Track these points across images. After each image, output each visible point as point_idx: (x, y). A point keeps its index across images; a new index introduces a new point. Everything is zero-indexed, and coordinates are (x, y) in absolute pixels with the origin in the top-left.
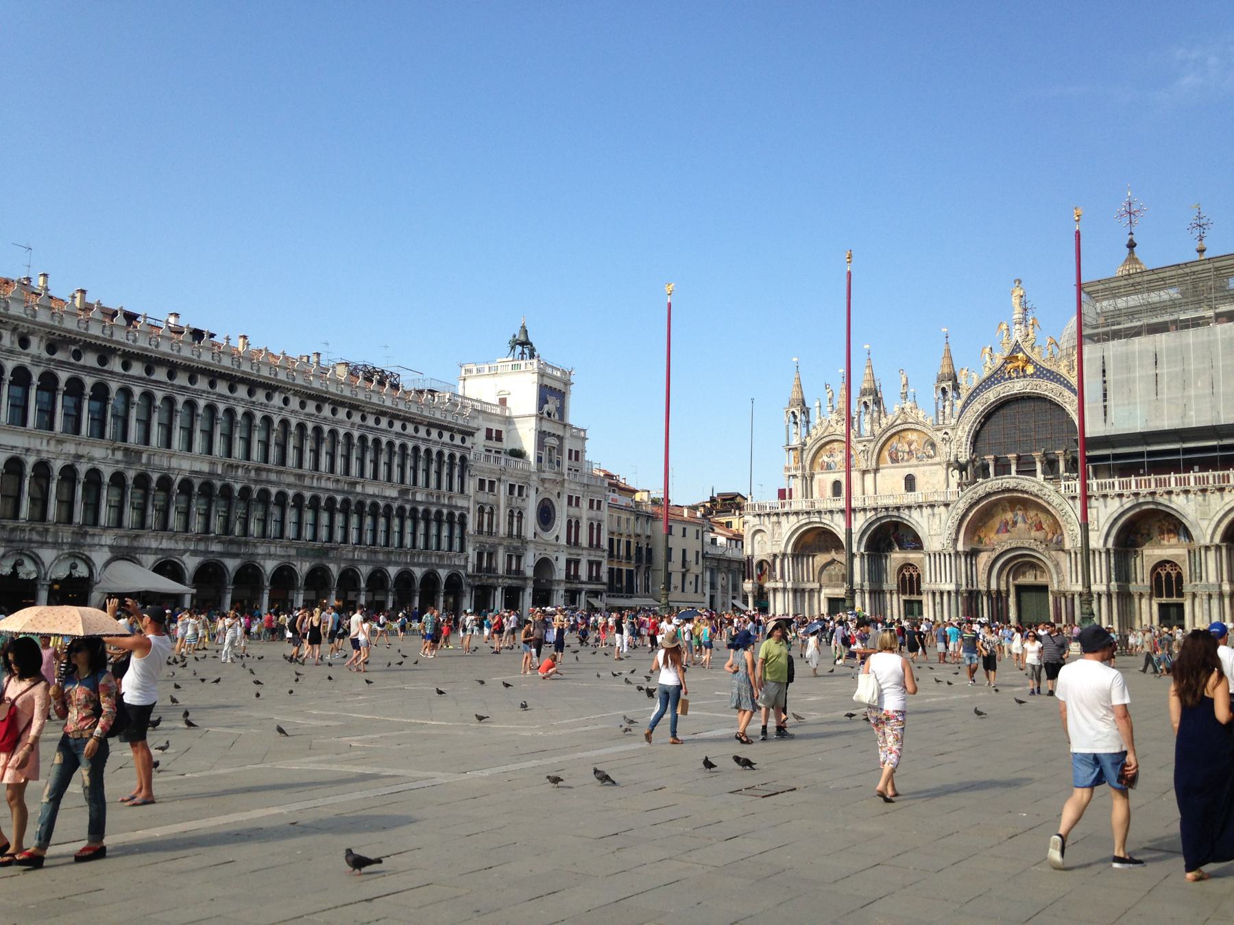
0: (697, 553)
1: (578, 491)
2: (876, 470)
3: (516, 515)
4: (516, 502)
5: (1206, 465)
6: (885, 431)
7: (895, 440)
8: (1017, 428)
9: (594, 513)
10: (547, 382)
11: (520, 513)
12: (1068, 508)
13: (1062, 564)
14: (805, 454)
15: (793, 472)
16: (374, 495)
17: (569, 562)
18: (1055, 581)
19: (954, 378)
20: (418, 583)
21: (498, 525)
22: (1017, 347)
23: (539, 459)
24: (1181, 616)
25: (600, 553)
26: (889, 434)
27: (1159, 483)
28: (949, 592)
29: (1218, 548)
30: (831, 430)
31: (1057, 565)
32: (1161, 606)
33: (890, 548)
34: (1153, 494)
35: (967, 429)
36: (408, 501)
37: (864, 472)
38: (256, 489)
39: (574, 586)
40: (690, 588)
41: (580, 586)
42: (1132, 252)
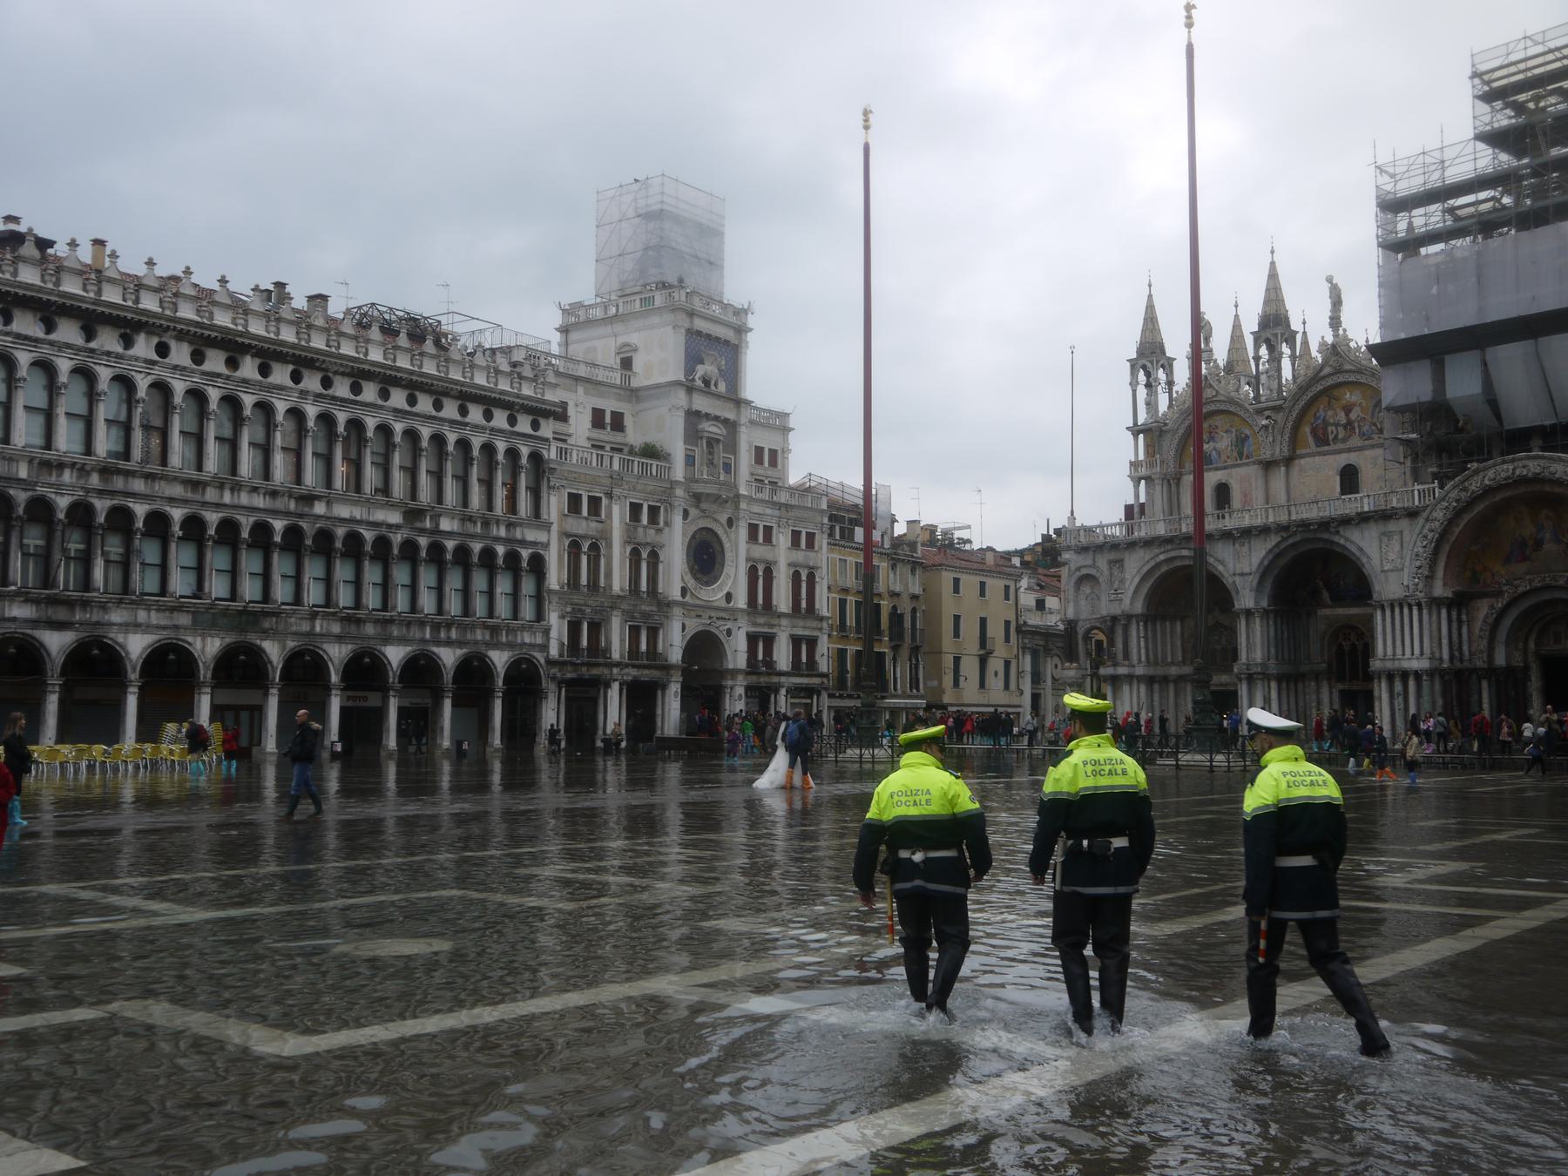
0: (1007, 623)
1: (768, 516)
2: (1288, 461)
3: (645, 557)
4: (646, 535)
6: (1302, 389)
7: (1321, 410)
9: (799, 556)
10: (700, 324)
11: (654, 555)
16: (352, 520)
17: (752, 639)
20: (448, 676)
21: (609, 575)
23: (690, 460)
25: (815, 624)
28: (1418, 675)
36: (422, 531)
37: (1268, 466)
38: (101, 506)
39: (763, 680)
40: (995, 683)
41: (775, 679)
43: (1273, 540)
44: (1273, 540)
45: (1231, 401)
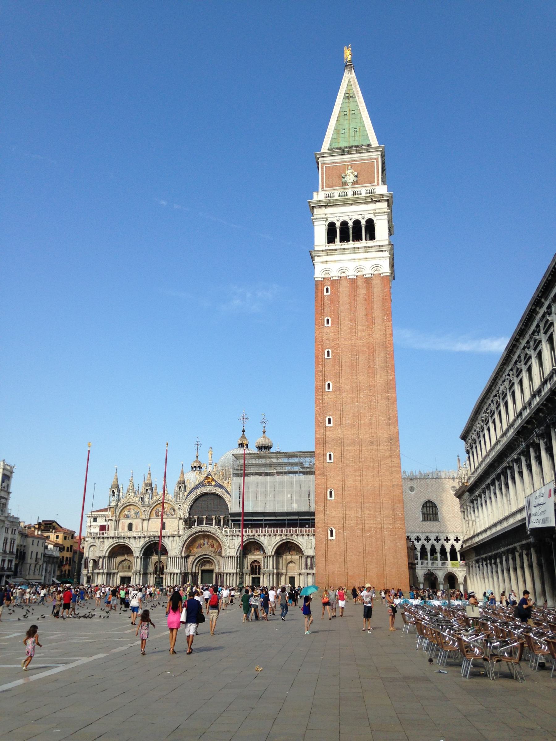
2: (149, 519)
5: (271, 526)
6: (155, 503)
8: (206, 507)
12: (225, 540)
13: (220, 562)
14: (117, 509)
15: (110, 518)
18: (217, 568)
19: (184, 483)
22: (209, 474)
24: (259, 582)
26: (156, 504)
27: (256, 532)
28: (177, 574)
29: (273, 556)
30: (130, 500)
31: (218, 562)
32: (252, 578)
33: (152, 554)
34: (254, 535)
35: (188, 504)
37: (144, 520)
42: (244, 434)
43: (147, 539)
44: (147, 539)
45: (136, 503)
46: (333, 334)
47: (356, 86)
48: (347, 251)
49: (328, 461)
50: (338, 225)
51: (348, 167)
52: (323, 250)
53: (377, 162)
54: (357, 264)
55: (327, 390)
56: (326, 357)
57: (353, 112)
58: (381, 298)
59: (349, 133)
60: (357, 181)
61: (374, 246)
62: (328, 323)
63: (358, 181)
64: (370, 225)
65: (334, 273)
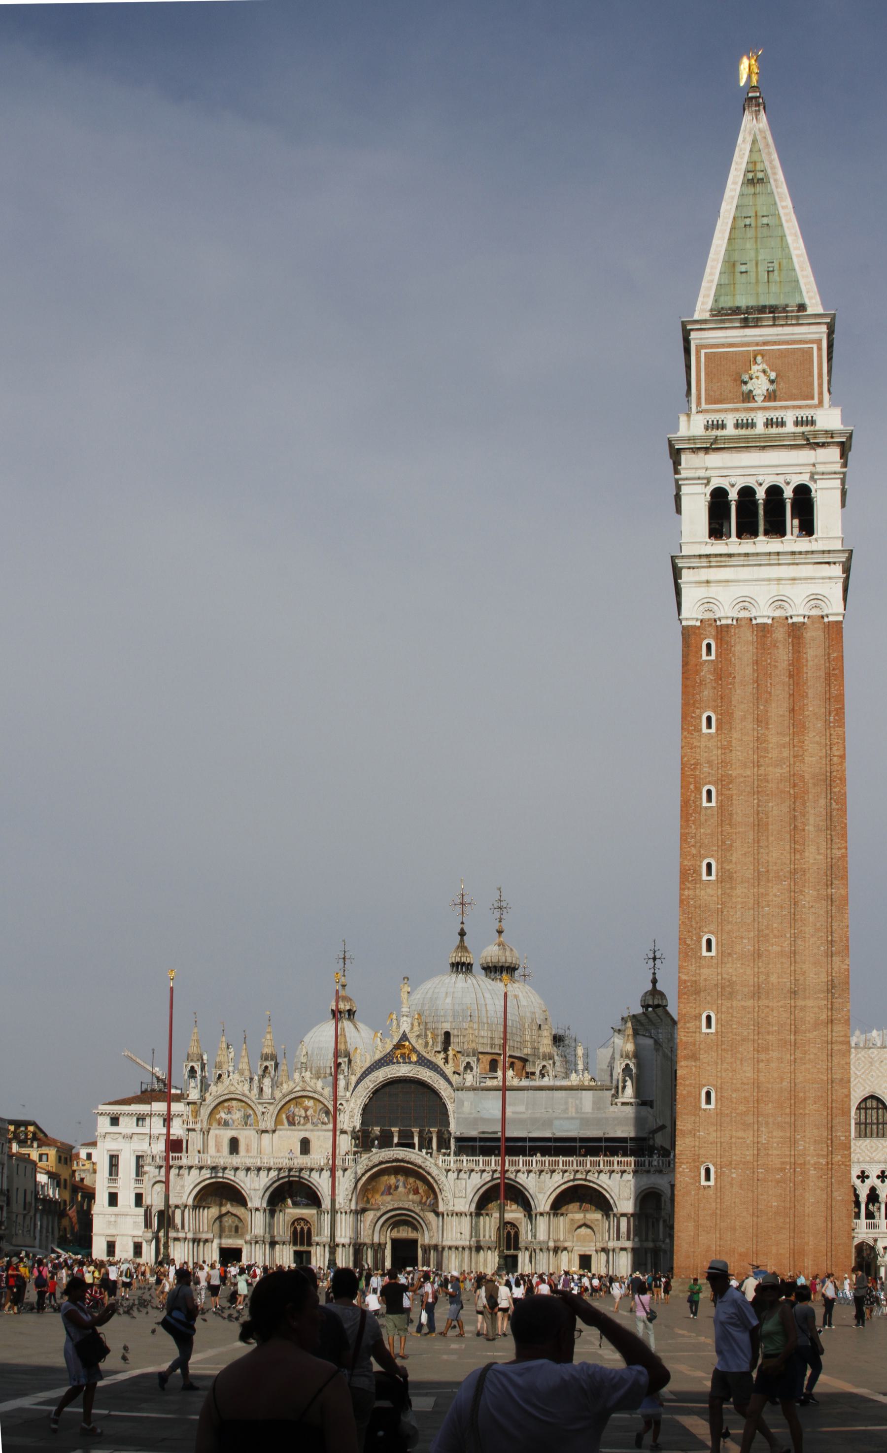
46: (720, 751)
47: (769, 154)
48: (752, 560)
49: (704, 1030)
50: (733, 495)
51: (755, 359)
52: (700, 556)
53: (820, 349)
54: (774, 590)
55: (705, 877)
56: (705, 804)
57: (765, 220)
58: (822, 674)
59: (757, 272)
60: (774, 391)
61: (813, 552)
62: (709, 726)
63: (778, 393)
64: (804, 499)
65: (726, 612)
